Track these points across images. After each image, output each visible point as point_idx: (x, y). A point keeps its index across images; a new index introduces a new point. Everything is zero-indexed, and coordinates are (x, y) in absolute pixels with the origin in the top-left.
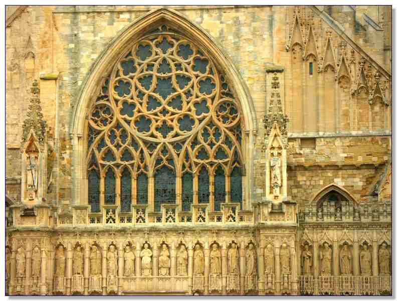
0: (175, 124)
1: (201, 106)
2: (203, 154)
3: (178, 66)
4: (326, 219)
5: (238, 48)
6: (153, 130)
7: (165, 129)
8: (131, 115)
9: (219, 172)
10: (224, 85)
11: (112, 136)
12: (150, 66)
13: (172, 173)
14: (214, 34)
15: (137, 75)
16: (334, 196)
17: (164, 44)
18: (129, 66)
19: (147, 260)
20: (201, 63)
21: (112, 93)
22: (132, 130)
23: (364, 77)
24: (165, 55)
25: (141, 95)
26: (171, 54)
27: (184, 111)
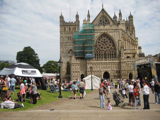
0: (106, 48)
1: (110, 45)
2: (110, 52)
3: (106, 40)
4: (129, 61)
5: (115, 37)
6: (103, 48)
7: (105, 48)
8: (100, 46)
9: (113, 54)
10: (113, 42)
11: (98, 49)
12: (102, 40)
13: (106, 55)
14: (111, 35)
15: (101, 41)
16: (128, 57)
17: (104, 37)
18: (99, 40)
19: (105, 66)
20: (109, 39)
21: (97, 43)
22: (100, 48)
23: (132, 41)
24: (105, 38)
25: (101, 44)
26: (105, 38)
27: (107, 46)
